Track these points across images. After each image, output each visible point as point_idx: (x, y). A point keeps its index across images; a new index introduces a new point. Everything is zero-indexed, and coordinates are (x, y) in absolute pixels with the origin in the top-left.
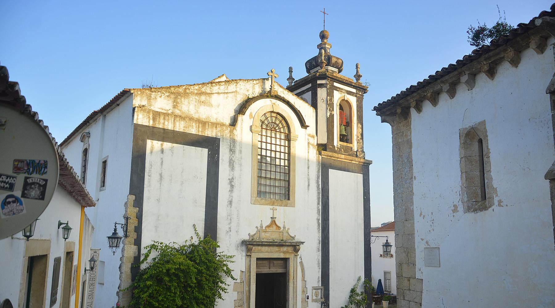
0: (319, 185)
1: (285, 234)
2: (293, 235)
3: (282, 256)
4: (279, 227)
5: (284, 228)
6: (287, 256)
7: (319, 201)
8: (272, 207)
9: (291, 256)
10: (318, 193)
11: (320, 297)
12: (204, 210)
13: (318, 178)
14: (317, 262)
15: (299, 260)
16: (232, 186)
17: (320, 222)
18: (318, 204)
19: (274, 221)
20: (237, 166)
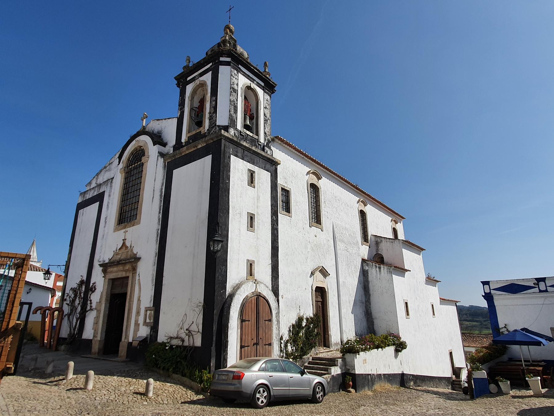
0: (162, 193)
1: (129, 253)
2: (135, 253)
3: (124, 274)
4: (127, 247)
5: (131, 247)
6: (128, 275)
7: (160, 210)
8: (124, 230)
9: (130, 275)
10: (161, 201)
11: (152, 321)
12: (91, 246)
13: (163, 184)
14: (151, 278)
15: (137, 278)
16: (106, 222)
17: (159, 232)
18: (160, 213)
19: (124, 244)
20: (110, 206)
